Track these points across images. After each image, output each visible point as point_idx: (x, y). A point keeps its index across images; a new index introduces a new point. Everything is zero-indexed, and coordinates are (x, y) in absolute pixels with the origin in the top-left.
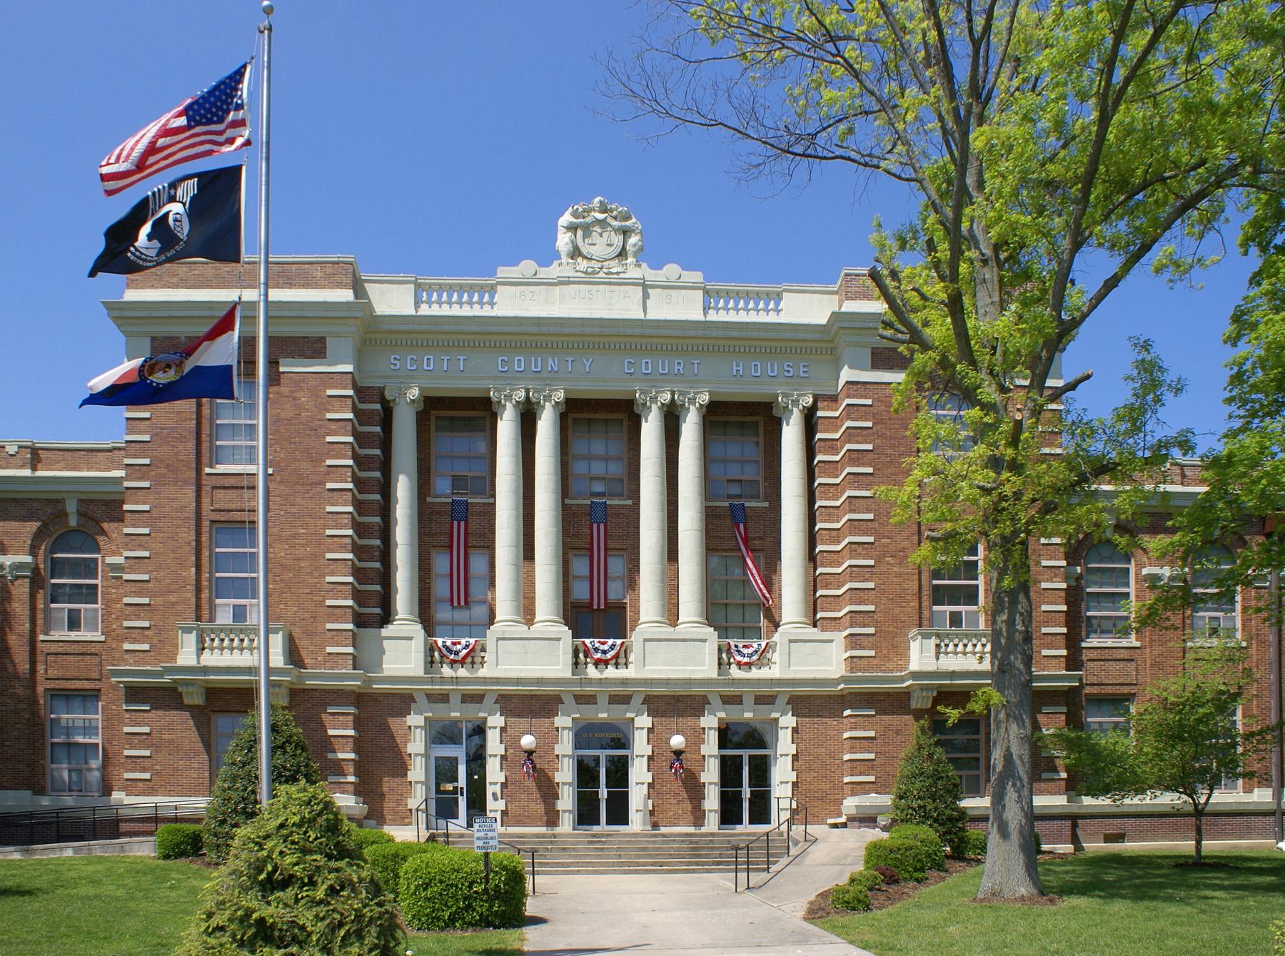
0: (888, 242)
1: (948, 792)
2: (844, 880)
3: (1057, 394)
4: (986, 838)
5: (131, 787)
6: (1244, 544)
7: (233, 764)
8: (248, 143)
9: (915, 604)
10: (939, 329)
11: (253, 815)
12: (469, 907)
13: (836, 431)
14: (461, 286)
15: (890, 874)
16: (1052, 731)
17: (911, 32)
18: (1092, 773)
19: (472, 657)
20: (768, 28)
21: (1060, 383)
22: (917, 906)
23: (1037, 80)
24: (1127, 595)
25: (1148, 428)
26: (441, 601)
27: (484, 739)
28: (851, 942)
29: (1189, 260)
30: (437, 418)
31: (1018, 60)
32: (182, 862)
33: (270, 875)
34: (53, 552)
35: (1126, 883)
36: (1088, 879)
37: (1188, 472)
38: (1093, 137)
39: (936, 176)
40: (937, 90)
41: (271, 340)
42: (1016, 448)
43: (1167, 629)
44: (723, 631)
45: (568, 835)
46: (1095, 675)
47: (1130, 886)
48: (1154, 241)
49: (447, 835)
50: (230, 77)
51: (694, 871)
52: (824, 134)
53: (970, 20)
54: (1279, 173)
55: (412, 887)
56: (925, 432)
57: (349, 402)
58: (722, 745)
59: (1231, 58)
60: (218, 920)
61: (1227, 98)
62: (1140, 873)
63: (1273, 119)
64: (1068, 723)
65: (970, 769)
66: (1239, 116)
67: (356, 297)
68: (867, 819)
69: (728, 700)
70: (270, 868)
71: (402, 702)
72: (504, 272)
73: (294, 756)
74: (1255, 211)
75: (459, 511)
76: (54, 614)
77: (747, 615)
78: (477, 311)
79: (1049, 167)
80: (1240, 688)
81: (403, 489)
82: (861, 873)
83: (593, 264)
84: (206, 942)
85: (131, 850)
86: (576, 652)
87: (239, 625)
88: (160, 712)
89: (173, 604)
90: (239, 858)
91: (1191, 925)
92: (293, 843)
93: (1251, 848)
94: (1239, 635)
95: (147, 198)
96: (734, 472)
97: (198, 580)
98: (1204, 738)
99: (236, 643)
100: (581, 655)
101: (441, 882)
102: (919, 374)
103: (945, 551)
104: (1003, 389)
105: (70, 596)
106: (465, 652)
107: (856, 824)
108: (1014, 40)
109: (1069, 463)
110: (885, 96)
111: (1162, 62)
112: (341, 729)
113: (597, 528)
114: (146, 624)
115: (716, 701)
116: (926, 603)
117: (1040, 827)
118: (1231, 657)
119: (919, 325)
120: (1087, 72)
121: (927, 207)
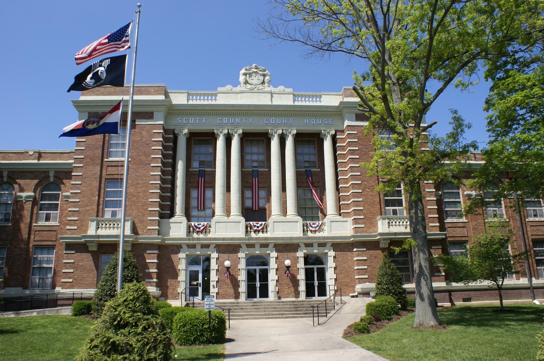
0: (359, 78)
1: (398, 281)
2: (358, 320)
3: (425, 129)
4: (415, 301)
5: (64, 285)
6: (502, 182)
7: (107, 275)
8: (129, 47)
9: (378, 206)
10: (380, 107)
11: (113, 296)
12: (202, 335)
13: (344, 143)
14: (204, 94)
15: (377, 317)
16: (437, 256)
17: (362, 12)
18: (455, 273)
19: (206, 230)
20: (313, 11)
21: (426, 125)
22: (389, 331)
23: (407, 26)
24: (460, 202)
25: (460, 140)
26: (195, 208)
27: (210, 263)
28: (363, 347)
29: (467, 83)
30: (194, 140)
31: (399, 20)
32: (82, 317)
33: (119, 322)
34: (43, 190)
35: (474, 319)
36: (458, 318)
37: (477, 156)
38: (428, 43)
39: (374, 56)
40: (373, 29)
41: (133, 113)
42: (412, 148)
43: (477, 215)
44: (305, 218)
45: (244, 303)
46: (452, 233)
47: (476, 320)
48: (454, 77)
49: (194, 303)
50: (124, 27)
51: (296, 317)
52: (334, 43)
53: (382, 8)
54: (494, 54)
55: (178, 326)
56: (377, 143)
57: (161, 134)
58: (306, 264)
59: (473, 19)
60: (95, 343)
61: (473, 31)
62: (479, 314)
63: (490, 38)
64: (443, 252)
65: (406, 272)
66: (478, 37)
67: (166, 98)
68: (366, 294)
69: (308, 245)
70: (119, 319)
71: (177, 248)
72: (220, 89)
73: (132, 271)
74: (487, 67)
75: (202, 174)
76: (40, 215)
77: (314, 212)
78: (210, 102)
79: (414, 53)
80: (508, 237)
81: (181, 166)
82: (365, 317)
83: (252, 86)
84: (89, 353)
85: (61, 312)
86: (247, 227)
87: (114, 218)
88: (79, 254)
89: (88, 210)
90: (106, 316)
91: (503, 337)
92: (129, 308)
93: (523, 303)
94: (505, 217)
95: (91, 66)
96: (306, 158)
97: (99, 201)
98: (497, 258)
99: (112, 225)
100: (249, 228)
101: (190, 324)
102: (373, 122)
103: (389, 186)
104: (405, 128)
105: (47, 208)
106: (203, 228)
107: (362, 296)
108: (397, 14)
109: (432, 153)
110: (355, 31)
111: (449, 20)
112: (152, 259)
113: (255, 180)
114: (76, 218)
115: (302, 246)
116: (383, 206)
117: (436, 296)
118: (503, 225)
119: (372, 106)
120: (424, 24)
121: (372, 66)
